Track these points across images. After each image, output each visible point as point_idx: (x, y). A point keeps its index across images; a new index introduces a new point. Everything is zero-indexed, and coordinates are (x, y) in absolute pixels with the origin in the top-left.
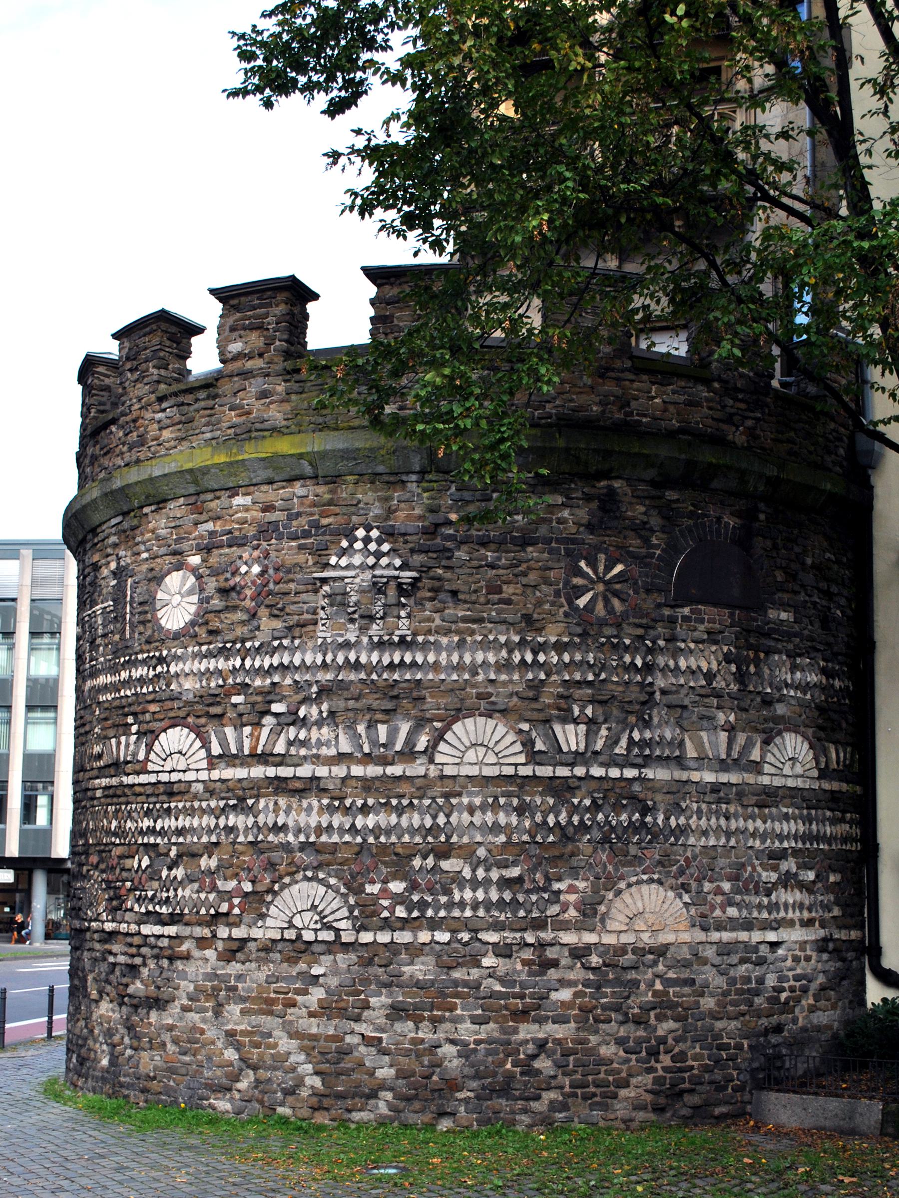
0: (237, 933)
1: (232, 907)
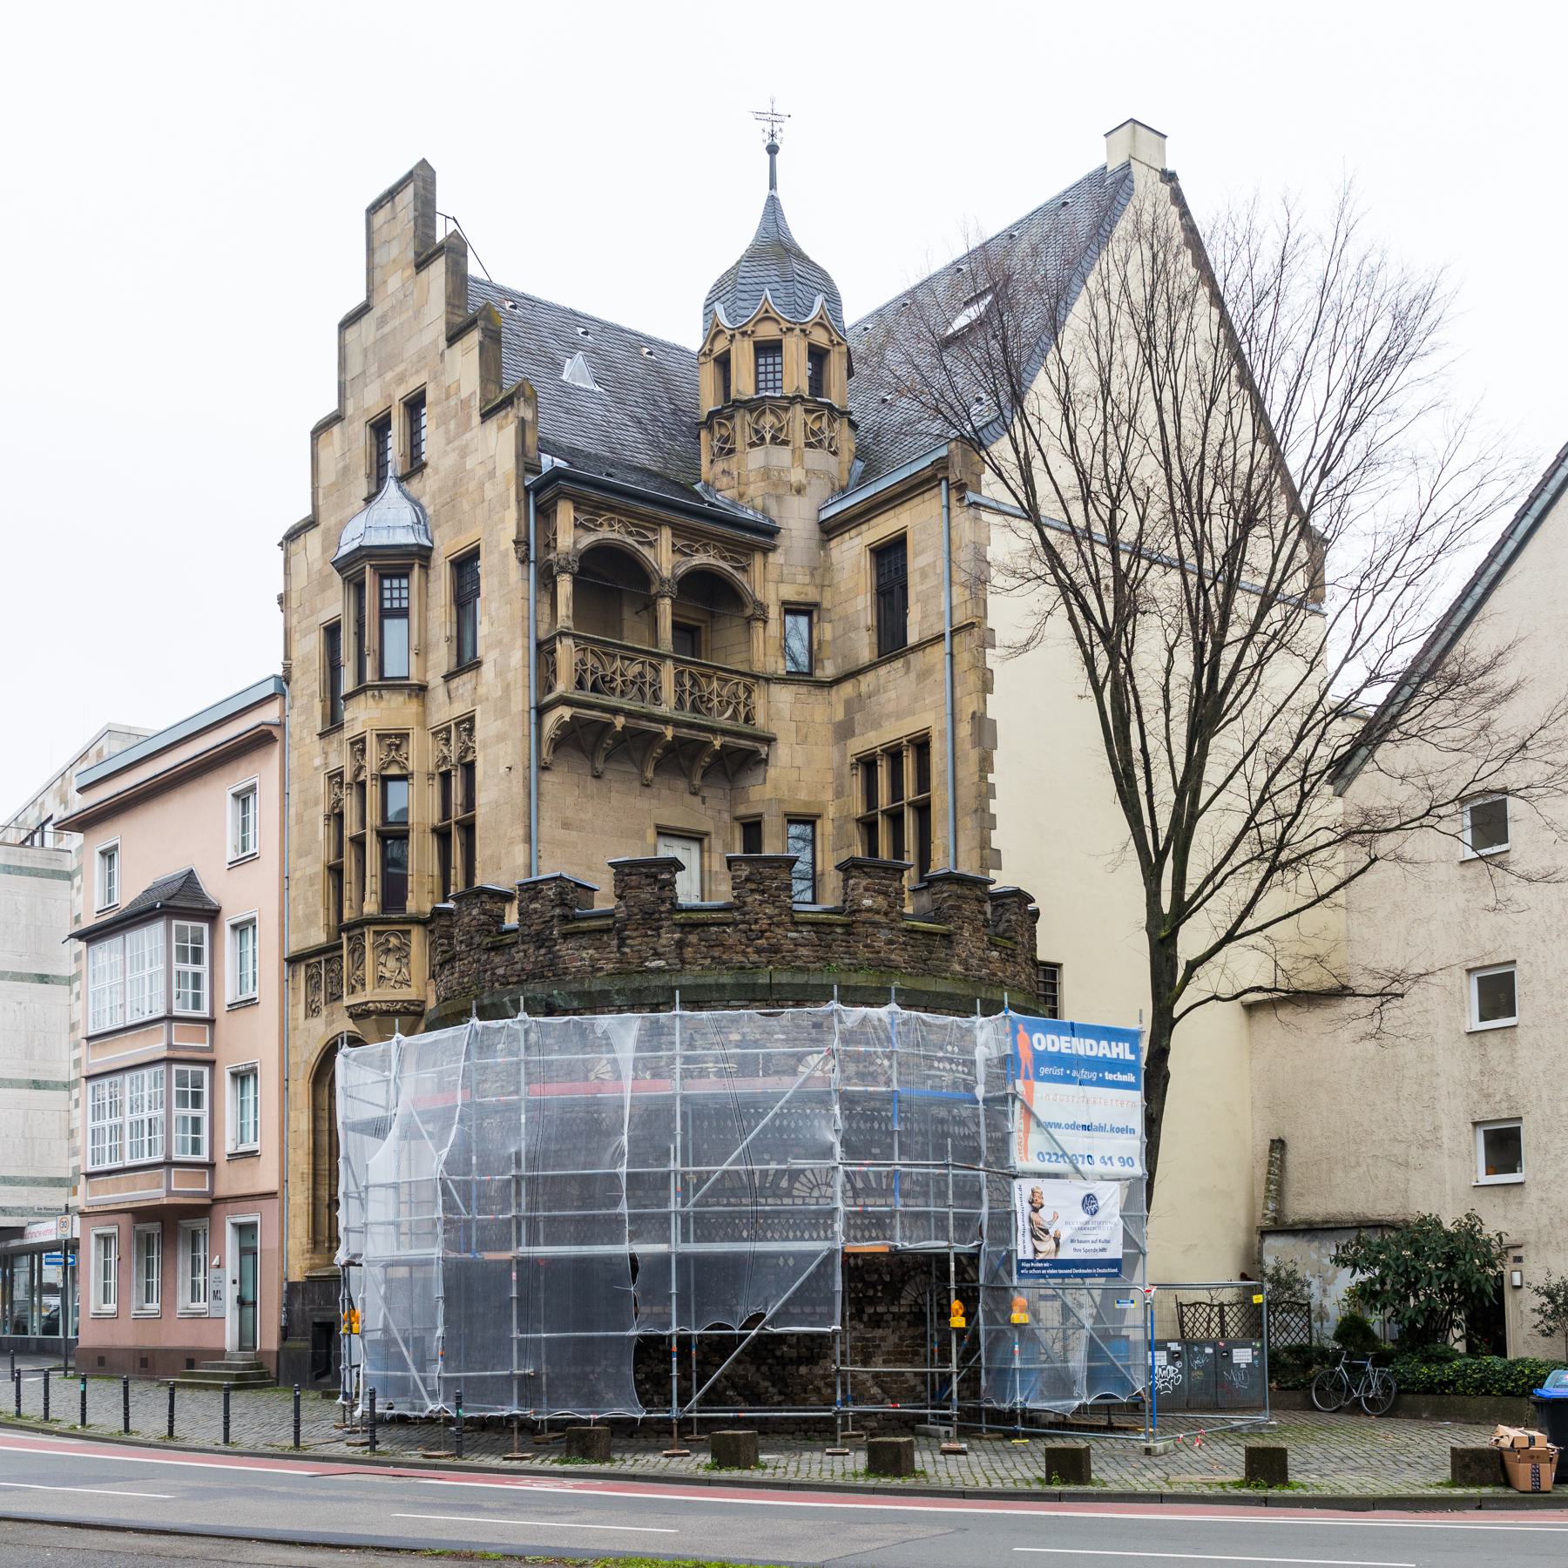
0: (880, 1309)
1: (876, 1291)
